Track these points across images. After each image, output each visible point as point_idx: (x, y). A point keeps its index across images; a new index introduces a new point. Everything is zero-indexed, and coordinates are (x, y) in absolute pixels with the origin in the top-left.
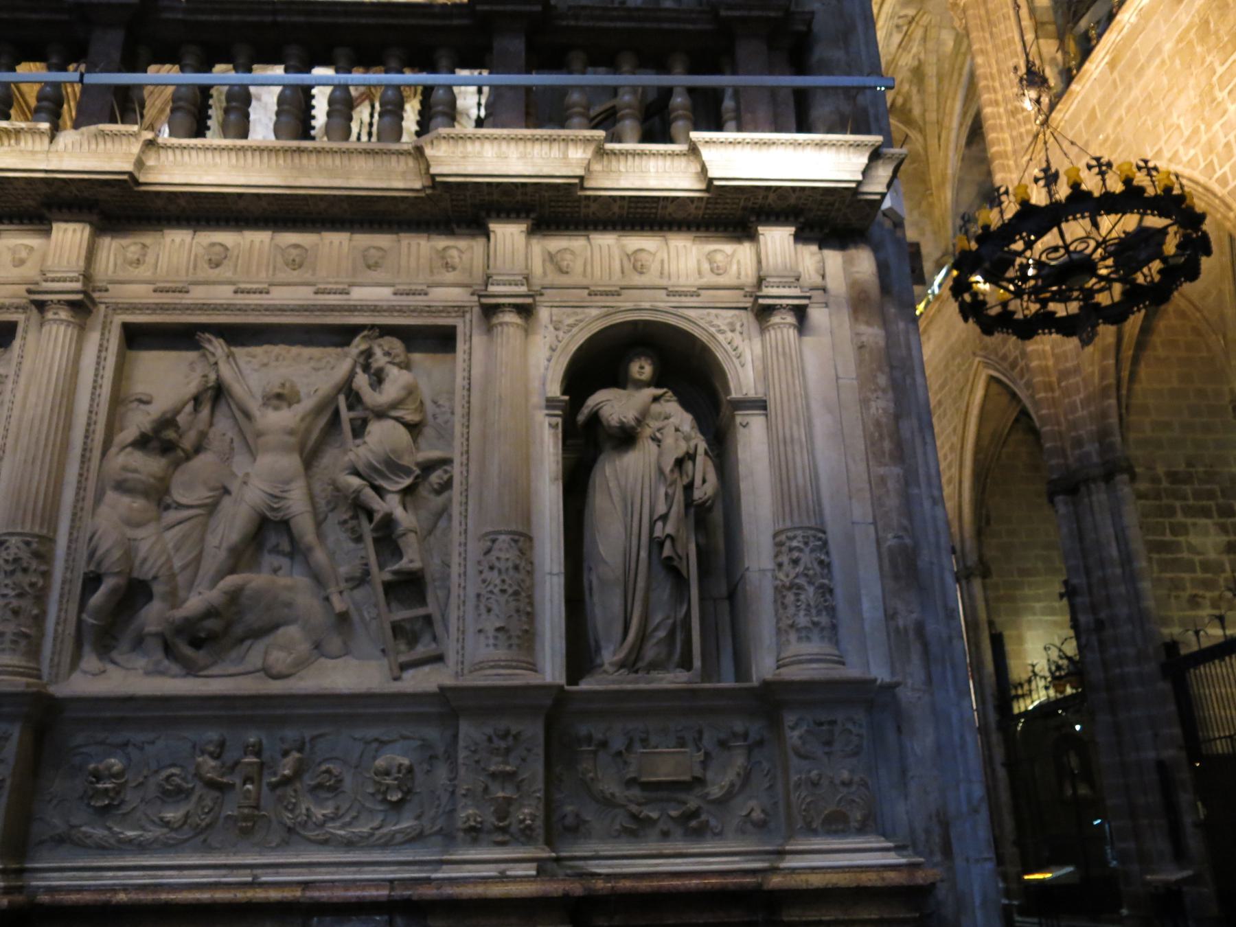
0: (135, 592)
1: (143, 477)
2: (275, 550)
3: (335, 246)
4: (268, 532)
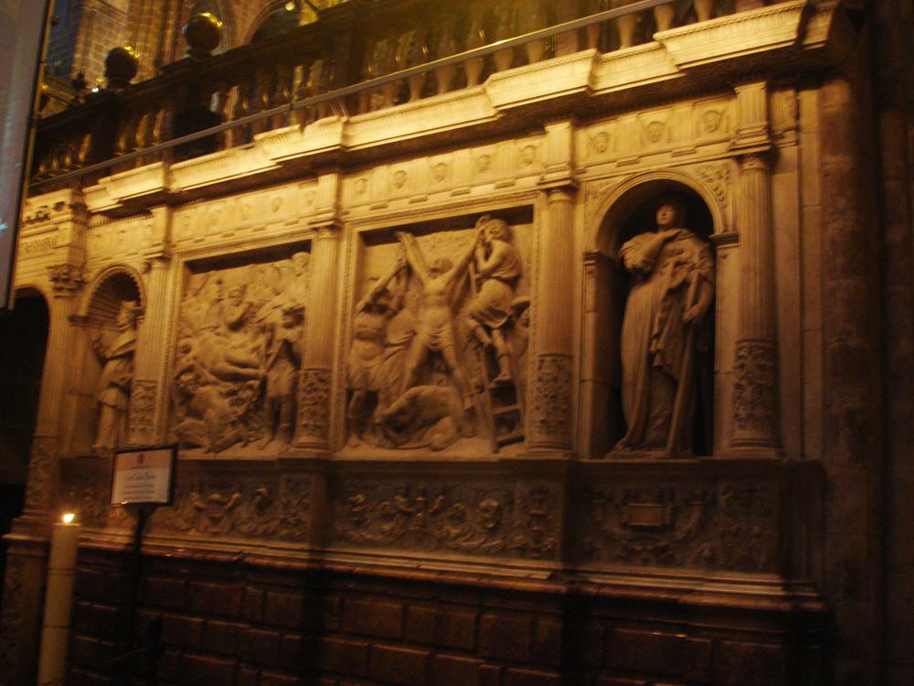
0: (371, 399)
1: (368, 330)
2: (439, 370)
3: (461, 159)
4: (432, 360)
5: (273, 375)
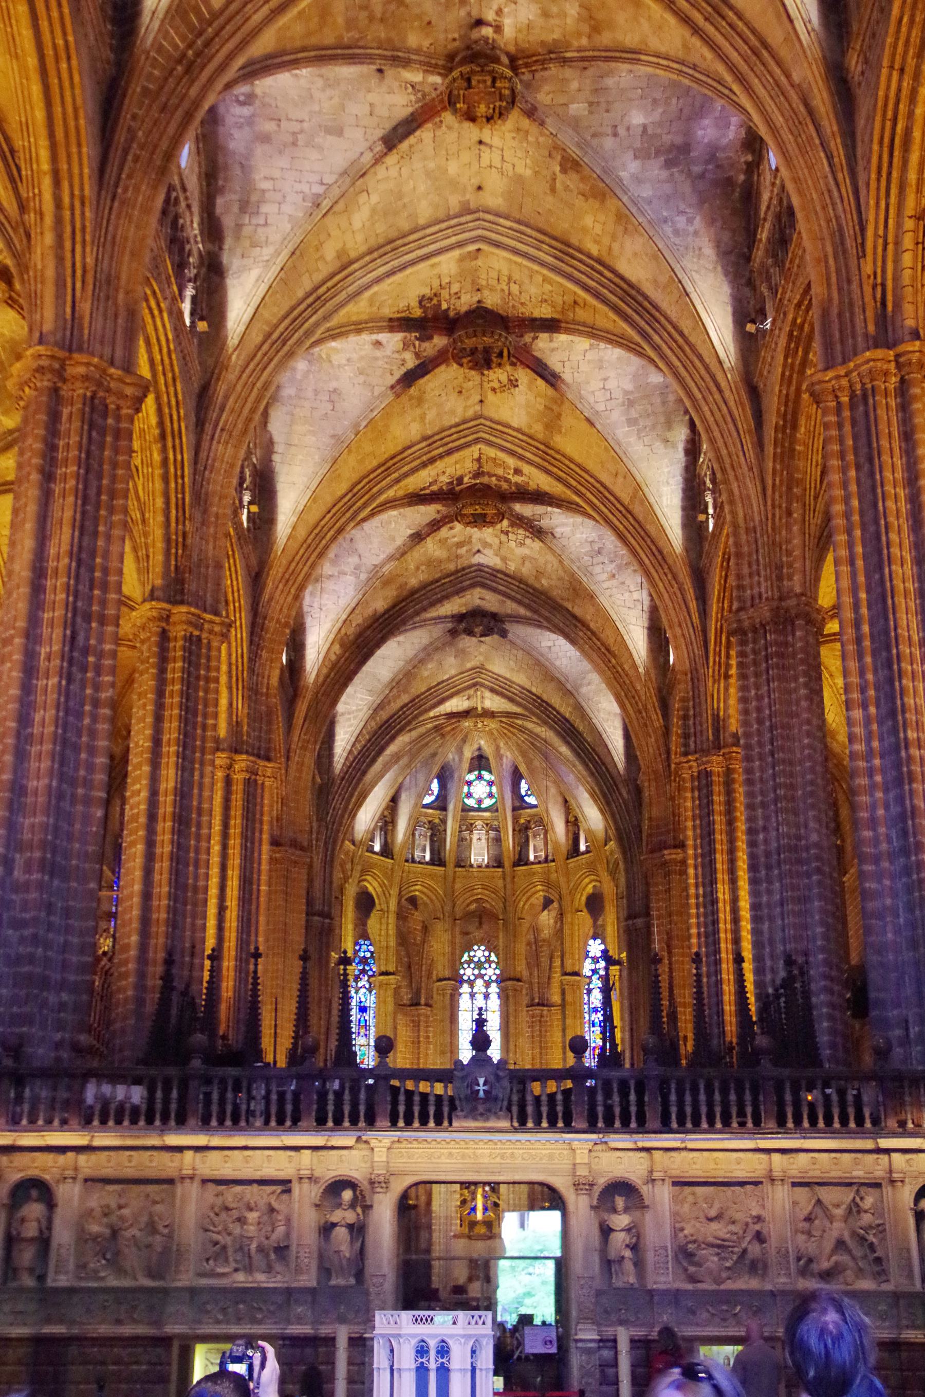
0: (810, 1261)
4: (840, 1244)
5: (750, 1248)
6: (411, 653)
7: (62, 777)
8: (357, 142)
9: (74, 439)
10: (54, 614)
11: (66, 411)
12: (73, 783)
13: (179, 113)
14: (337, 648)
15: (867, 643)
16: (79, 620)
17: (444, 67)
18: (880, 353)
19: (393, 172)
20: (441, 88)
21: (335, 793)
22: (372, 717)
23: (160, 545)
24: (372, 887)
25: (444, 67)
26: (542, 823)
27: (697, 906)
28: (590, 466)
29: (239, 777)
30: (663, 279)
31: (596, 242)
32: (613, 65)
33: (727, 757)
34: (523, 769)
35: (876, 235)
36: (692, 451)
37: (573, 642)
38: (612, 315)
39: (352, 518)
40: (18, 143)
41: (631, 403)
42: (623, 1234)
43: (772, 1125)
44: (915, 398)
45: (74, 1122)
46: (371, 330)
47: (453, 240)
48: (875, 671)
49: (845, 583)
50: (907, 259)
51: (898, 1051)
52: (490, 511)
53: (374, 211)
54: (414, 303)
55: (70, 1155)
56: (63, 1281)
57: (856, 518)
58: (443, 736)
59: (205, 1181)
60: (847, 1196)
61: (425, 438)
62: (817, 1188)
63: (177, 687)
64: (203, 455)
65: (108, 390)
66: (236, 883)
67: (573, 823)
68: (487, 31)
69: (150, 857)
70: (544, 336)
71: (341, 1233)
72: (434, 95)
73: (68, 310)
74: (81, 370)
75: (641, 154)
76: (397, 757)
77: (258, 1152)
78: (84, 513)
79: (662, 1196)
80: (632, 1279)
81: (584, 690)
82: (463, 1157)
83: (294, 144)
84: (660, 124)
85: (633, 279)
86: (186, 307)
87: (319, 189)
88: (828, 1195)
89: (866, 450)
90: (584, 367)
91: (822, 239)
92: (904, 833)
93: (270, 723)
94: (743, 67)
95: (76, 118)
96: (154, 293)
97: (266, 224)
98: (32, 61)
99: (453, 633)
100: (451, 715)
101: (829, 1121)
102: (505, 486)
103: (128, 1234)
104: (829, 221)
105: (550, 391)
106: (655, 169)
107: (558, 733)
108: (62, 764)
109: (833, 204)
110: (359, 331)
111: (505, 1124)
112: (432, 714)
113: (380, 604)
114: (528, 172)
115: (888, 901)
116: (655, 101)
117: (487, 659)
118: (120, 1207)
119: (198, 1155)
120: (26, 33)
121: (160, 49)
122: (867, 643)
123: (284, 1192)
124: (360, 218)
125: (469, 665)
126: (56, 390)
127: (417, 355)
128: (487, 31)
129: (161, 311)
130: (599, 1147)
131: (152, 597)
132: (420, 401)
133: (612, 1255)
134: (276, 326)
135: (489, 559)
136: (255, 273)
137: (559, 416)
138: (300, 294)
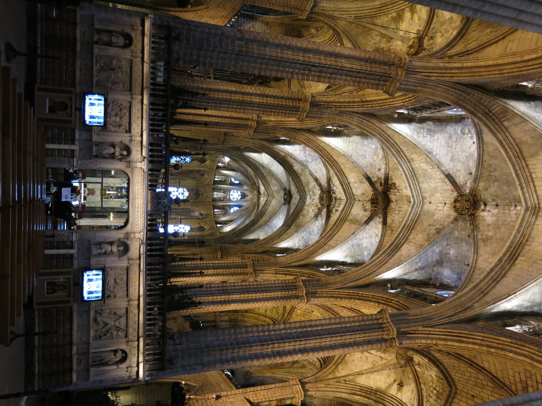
0: (100, 314)
4: (106, 324)
6: (279, 176)
7: (269, 59)
8: (448, 166)
9: (378, 70)
10: (323, 60)
11: (386, 68)
12: (267, 64)
13: (473, 110)
14: (283, 154)
15: (305, 330)
16: (320, 68)
17: (472, 193)
18: (395, 333)
19: (438, 177)
20: (464, 192)
21: (237, 153)
22: (260, 164)
23: (328, 100)
24: (208, 163)
25: (472, 193)
26: (226, 213)
27: (206, 264)
28: (340, 233)
29: (249, 123)
30: (402, 258)
31: (413, 238)
32: (473, 246)
33: (251, 273)
34: (242, 208)
35: (430, 331)
36: (344, 264)
37: (283, 225)
38: (391, 242)
39: (326, 160)
40: (471, 56)
41: (358, 246)
42: (110, 249)
43: (148, 301)
44: (381, 345)
45: (152, 57)
46: (386, 168)
47: (414, 194)
48: (295, 332)
49: (323, 322)
50: (424, 341)
51: (172, 342)
52: (324, 202)
53: (426, 170)
54: (393, 181)
55: (141, 55)
56: (96, 50)
57: (344, 325)
58: (252, 185)
59: (130, 102)
60: (123, 326)
61: (349, 183)
62: (126, 316)
63: (284, 103)
64: (355, 115)
65: (392, 82)
66: (217, 121)
67: (226, 223)
68: (483, 207)
69: (231, 92)
70: (381, 220)
71: (112, 150)
72: (463, 190)
73: (418, 70)
74: (400, 73)
75: (441, 253)
76: (247, 171)
77: (140, 122)
78: (354, 72)
79: (124, 263)
80: (94, 252)
81: (267, 228)
82: (138, 194)
83: (448, 146)
84: (450, 258)
85: (401, 249)
86: (401, 111)
87: (434, 154)
88: (123, 320)
89: (365, 328)
90: (370, 232)
91: (428, 313)
92: (243, 343)
93: (265, 133)
94: (479, 288)
95: (479, 76)
96: (410, 100)
97: (424, 137)
98: (500, 62)
99: (285, 189)
100: (259, 188)
101: (148, 320)
102: (332, 206)
103: (113, 75)
104: (433, 315)
105: (363, 222)
106: (436, 257)
107: (253, 220)
108: (274, 60)
109: (438, 317)
110: (386, 165)
111: (149, 209)
112: (260, 182)
113: (297, 167)
114: (436, 218)
115: (221, 338)
116: (457, 257)
117: (276, 199)
118: (122, 72)
119: (140, 101)
120: (510, 60)
121: (494, 104)
122: (305, 330)
123: (126, 130)
124: (424, 166)
125: (274, 194)
126: (394, 65)
127: (376, 182)
128: (483, 207)
129: (403, 102)
130: (141, 241)
131: (313, 96)
132: (361, 182)
133: (103, 246)
134: (392, 139)
135: (308, 201)
136: (409, 133)
137: (355, 224)
138: (401, 147)
